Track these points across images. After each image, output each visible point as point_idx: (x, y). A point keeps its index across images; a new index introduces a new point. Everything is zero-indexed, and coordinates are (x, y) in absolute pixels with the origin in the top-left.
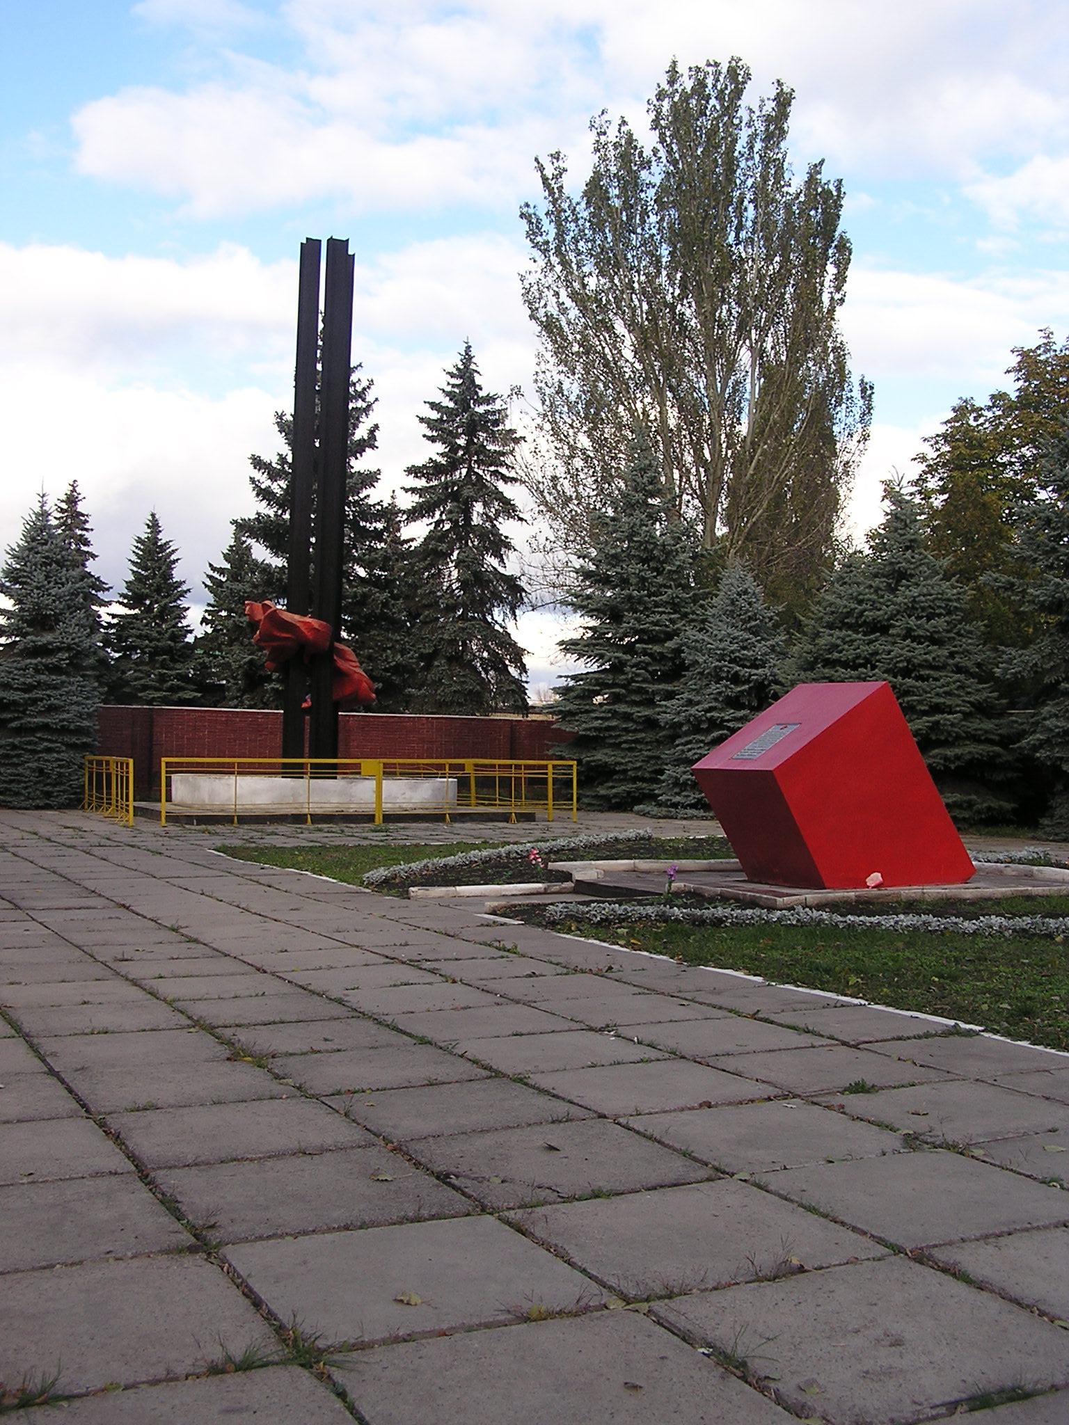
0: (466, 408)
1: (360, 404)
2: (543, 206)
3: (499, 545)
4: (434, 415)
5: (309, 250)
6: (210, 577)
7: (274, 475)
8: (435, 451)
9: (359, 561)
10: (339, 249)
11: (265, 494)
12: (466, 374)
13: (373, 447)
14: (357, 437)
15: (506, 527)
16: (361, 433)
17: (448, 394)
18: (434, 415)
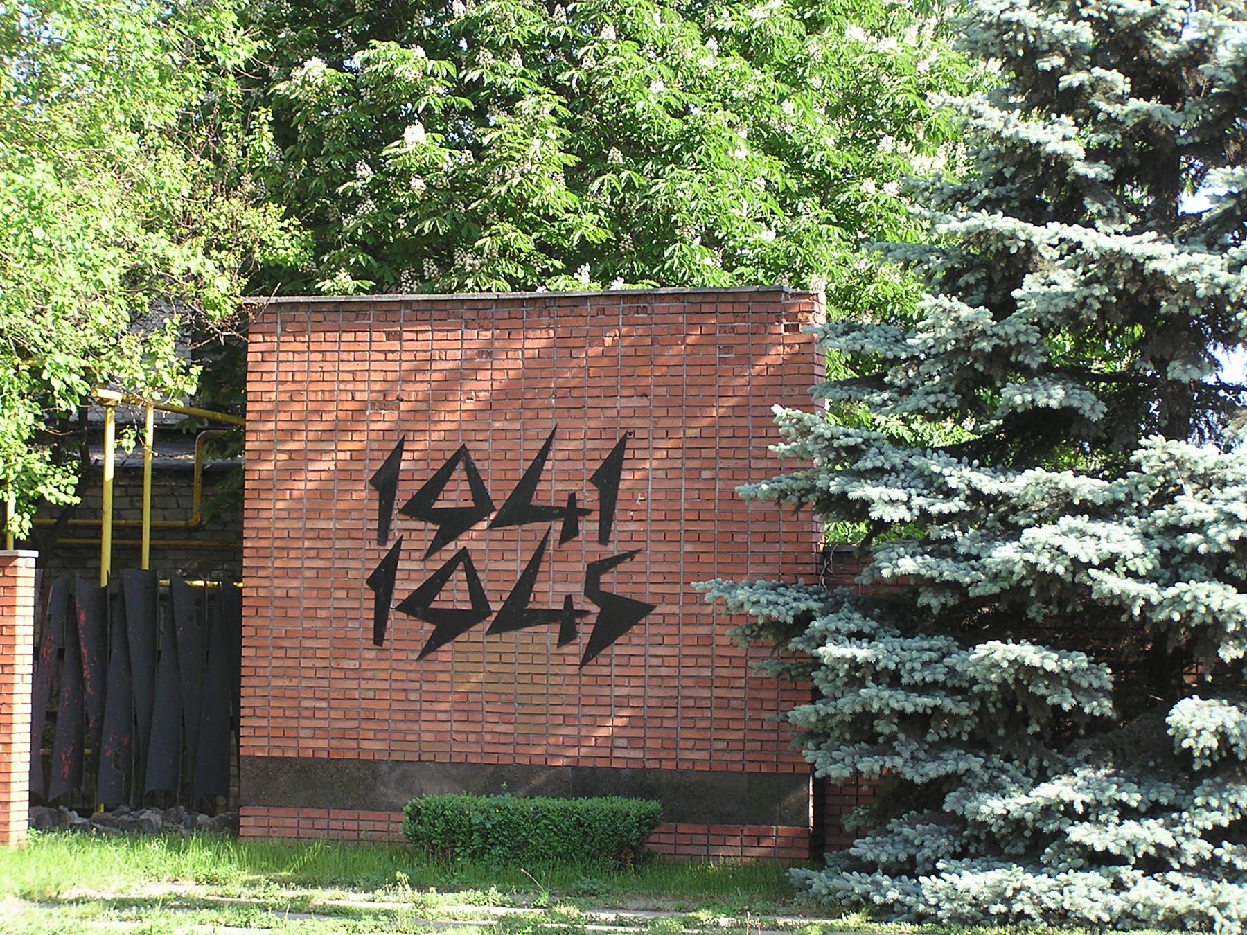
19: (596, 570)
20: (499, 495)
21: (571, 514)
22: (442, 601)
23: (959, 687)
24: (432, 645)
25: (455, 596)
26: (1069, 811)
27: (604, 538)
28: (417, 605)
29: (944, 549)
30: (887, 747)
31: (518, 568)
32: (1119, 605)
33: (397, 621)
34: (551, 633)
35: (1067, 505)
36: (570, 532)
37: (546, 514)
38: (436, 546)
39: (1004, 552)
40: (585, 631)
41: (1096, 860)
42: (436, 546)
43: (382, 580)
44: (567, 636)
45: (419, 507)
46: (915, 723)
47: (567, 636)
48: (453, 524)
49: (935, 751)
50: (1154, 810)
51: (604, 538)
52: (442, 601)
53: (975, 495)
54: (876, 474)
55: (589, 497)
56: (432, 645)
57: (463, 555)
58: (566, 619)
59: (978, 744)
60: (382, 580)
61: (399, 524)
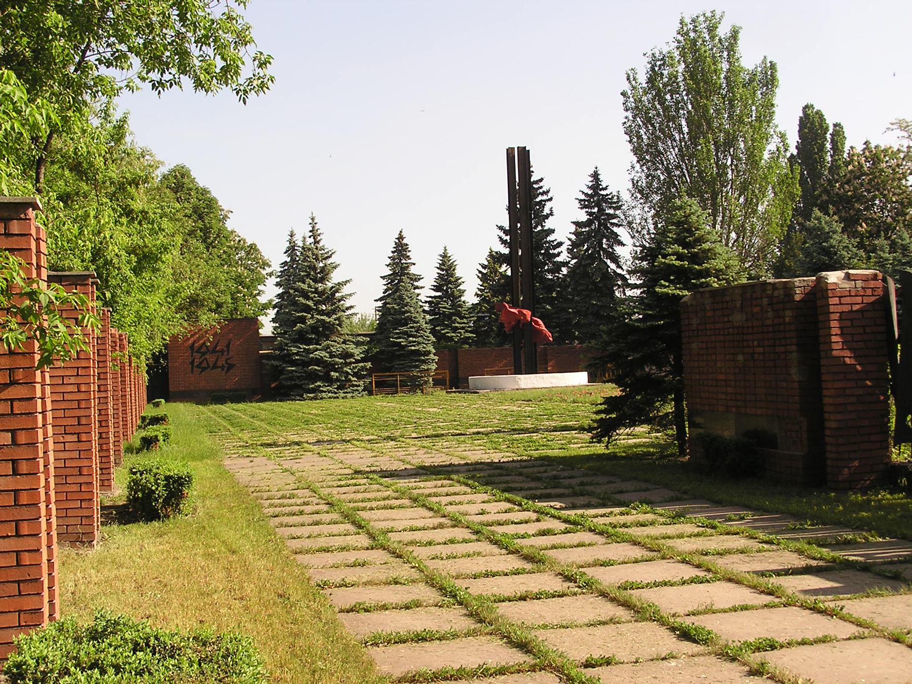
0: (596, 193)
1: (545, 197)
2: (626, 87)
3: (615, 259)
4: (583, 197)
5: (510, 152)
6: (480, 272)
7: (506, 232)
8: (583, 217)
9: (549, 271)
10: (524, 154)
11: (503, 242)
12: (596, 176)
13: (552, 215)
14: (545, 214)
15: (618, 250)
16: (546, 211)
17: (589, 187)
18: (583, 197)
19: (227, 360)
20: (211, 350)
21: (222, 351)
22: (202, 366)
23: (305, 372)
24: (201, 372)
25: (205, 365)
26: (320, 386)
27: (228, 355)
28: (198, 366)
29: (301, 355)
30: (295, 380)
31: (214, 360)
32: (326, 361)
33: (195, 368)
34: (220, 370)
35: (317, 350)
36: (222, 354)
37: (218, 352)
38: (201, 357)
39: (311, 355)
40: (225, 369)
41: (325, 392)
42: (201, 357)
43: (192, 363)
44: (223, 370)
45: (198, 351)
46: (298, 377)
47: (223, 370)
48: (204, 354)
49: (300, 381)
50: (328, 386)
51: (228, 355)
52: (202, 366)
53: (304, 349)
54: (291, 347)
55: (225, 349)
56: (201, 372)
57: (206, 358)
58: (222, 367)
59: (306, 379)
60: (192, 363)
61: (195, 354)
